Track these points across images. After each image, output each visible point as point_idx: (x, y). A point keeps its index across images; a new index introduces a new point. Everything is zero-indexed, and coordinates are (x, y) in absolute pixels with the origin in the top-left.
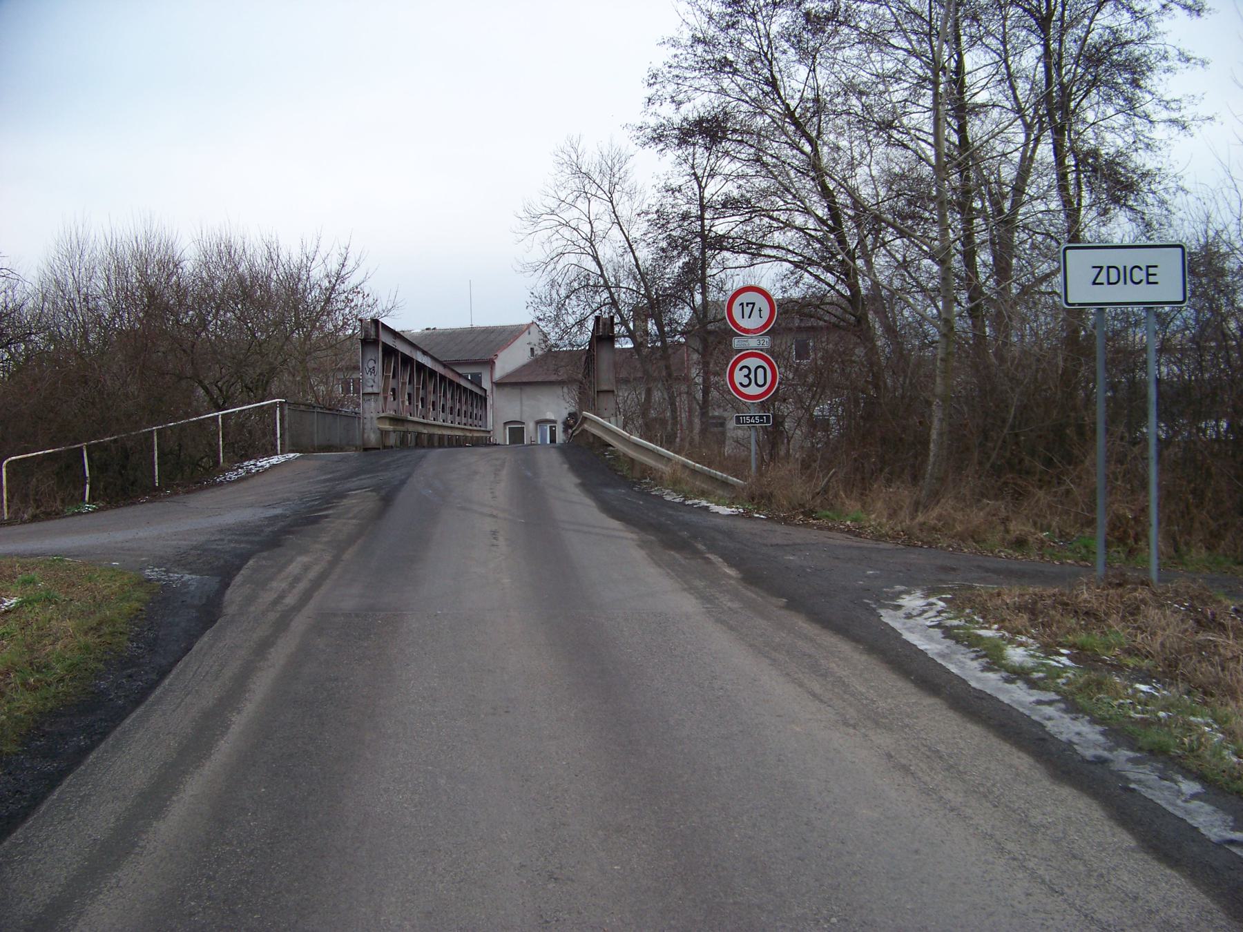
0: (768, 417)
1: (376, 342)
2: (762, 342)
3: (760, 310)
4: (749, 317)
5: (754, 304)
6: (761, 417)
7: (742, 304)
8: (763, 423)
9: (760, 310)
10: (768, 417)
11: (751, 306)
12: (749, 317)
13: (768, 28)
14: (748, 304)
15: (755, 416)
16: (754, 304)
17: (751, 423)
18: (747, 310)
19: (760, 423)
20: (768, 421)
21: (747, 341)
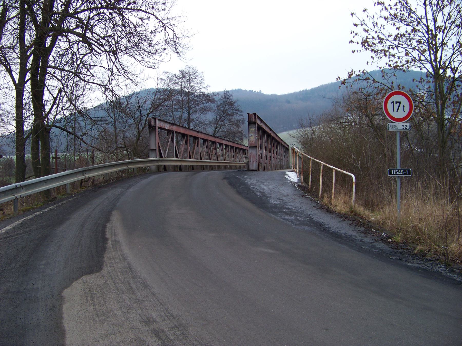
0: (409, 171)
1: (255, 123)
2: (405, 127)
3: (404, 107)
4: (397, 111)
5: (400, 102)
6: (405, 171)
7: (393, 102)
8: (406, 174)
9: (404, 107)
10: (409, 171)
11: (398, 104)
12: (397, 111)
13: (174, 34)
14: (396, 102)
15: (401, 170)
16: (400, 102)
17: (398, 174)
18: (396, 106)
19: (404, 174)
20: (409, 174)
21: (396, 126)
